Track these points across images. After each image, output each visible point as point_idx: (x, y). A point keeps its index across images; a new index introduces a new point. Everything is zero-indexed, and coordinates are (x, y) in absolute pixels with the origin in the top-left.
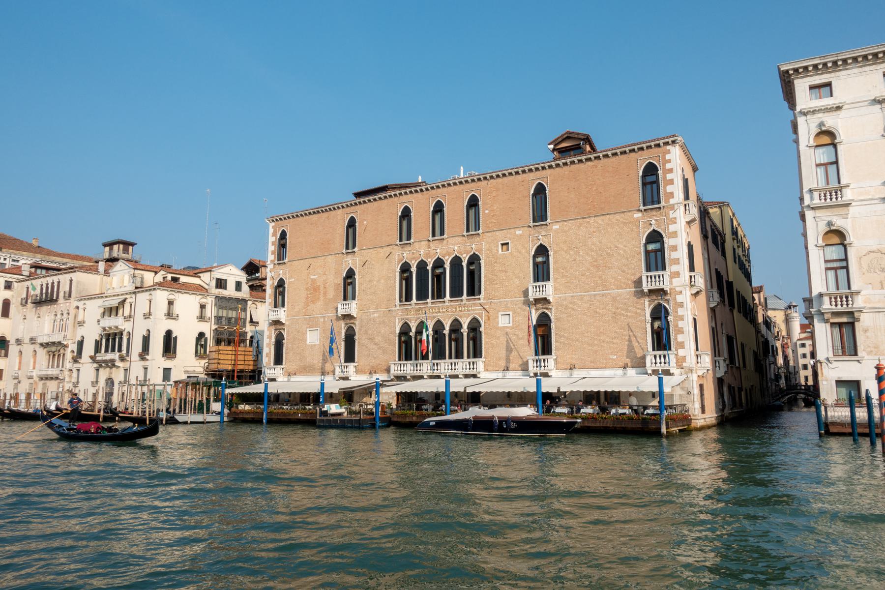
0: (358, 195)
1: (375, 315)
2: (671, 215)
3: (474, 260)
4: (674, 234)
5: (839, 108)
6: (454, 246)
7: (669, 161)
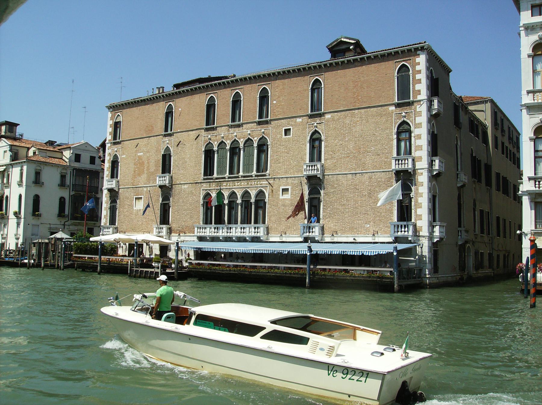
0: (177, 86)
1: (186, 186)
2: (418, 110)
4: (419, 126)
6: (249, 131)
7: (419, 64)
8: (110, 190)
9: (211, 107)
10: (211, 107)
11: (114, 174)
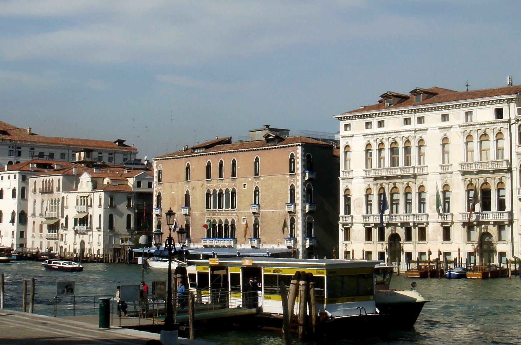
6: (226, 184)
8: (157, 215)
9: (208, 167)
10: (208, 167)
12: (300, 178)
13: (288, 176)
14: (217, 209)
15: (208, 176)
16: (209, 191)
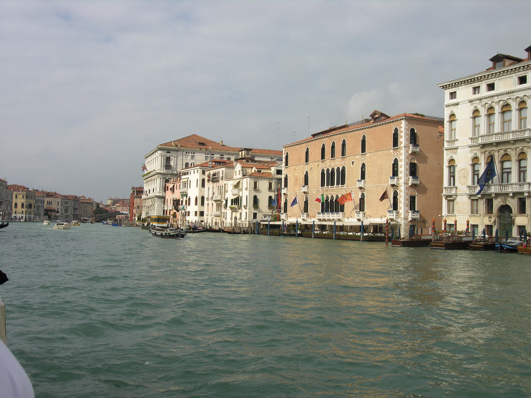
0: (314, 136)
3: (344, 168)
5: (457, 104)
9: (323, 150)
10: (323, 150)
11: (286, 186)
12: (403, 151)
13: (392, 151)
14: (340, 185)
15: (323, 157)
16: (323, 170)
